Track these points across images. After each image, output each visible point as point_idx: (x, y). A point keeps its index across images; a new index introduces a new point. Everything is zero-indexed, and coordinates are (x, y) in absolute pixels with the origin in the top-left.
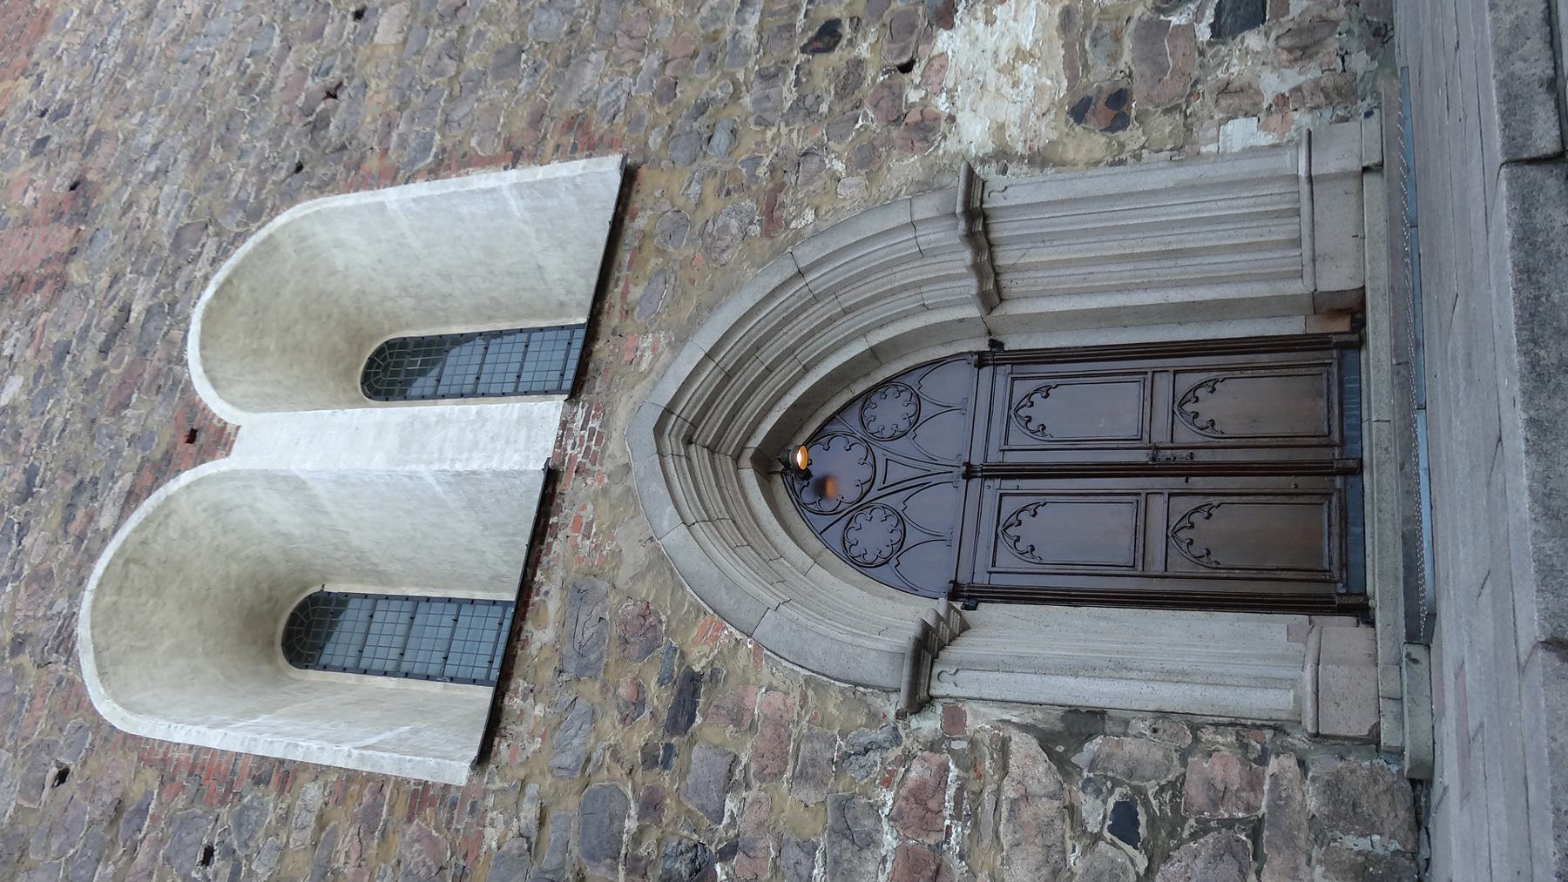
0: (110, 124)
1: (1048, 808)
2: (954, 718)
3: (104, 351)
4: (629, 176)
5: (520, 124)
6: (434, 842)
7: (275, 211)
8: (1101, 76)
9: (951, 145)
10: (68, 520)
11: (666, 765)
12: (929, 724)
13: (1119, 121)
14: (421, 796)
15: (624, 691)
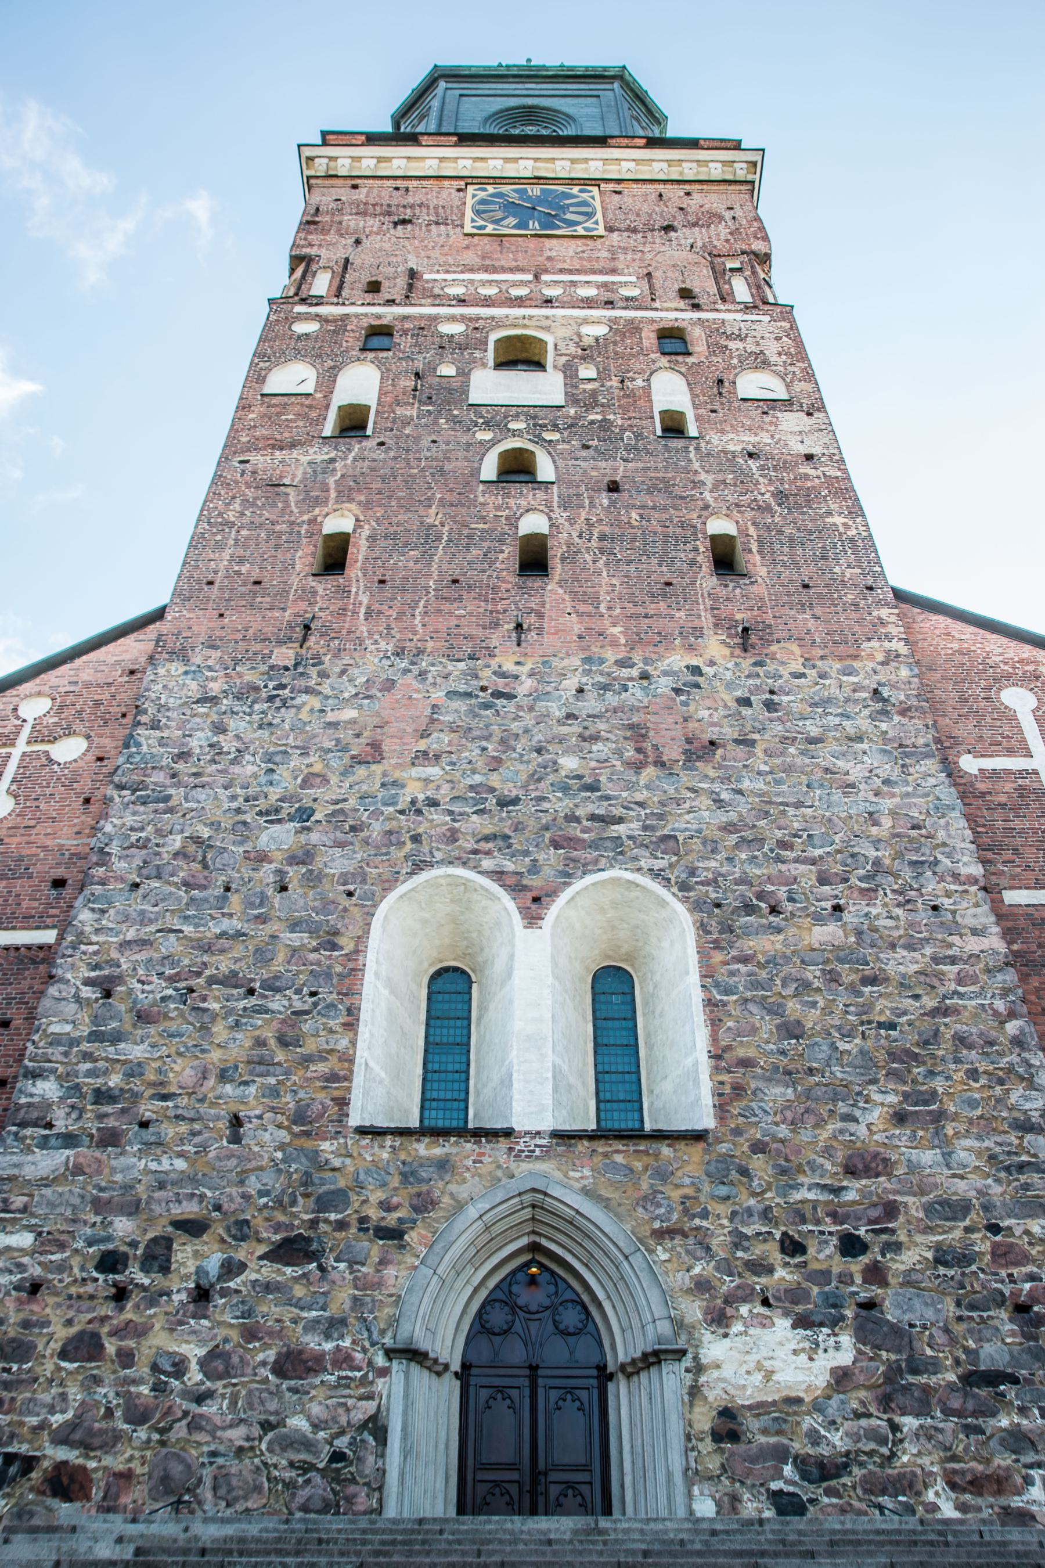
0: (759, 751)
1: (343, 1420)
2: (384, 1372)
3: (593, 817)
4: (698, 1136)
5: (741, 1053)
6: (322, 1115)
7: (685, 900)
8: (752, 1424)
9: (707, 1336)
10: (487, 838)
11: (360, 1230)
12: (380, 1361)
13: (717, 1436)
14: (343, 1103)
15: (395, 1200)
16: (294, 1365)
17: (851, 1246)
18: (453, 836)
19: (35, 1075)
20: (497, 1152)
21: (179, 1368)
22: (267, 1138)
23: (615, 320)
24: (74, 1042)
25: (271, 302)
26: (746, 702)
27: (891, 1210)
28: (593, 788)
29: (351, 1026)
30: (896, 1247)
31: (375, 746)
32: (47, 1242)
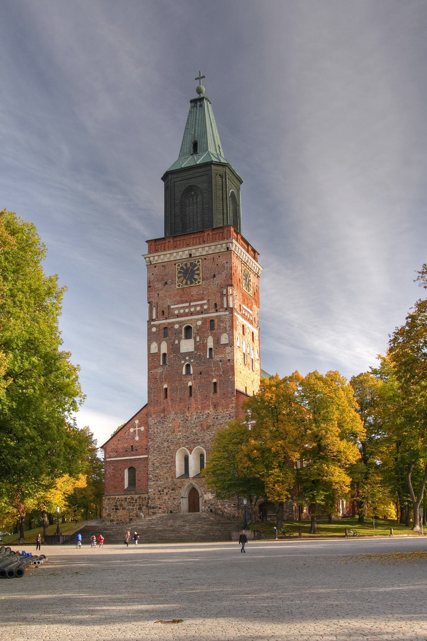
14: (175, 475)
16: (174, 499)
20: (188, 479)
21: (166, 499)
23: (203, 319)
25: (147, 321)
26: (214, 418)
28: (196, 434)
29: (175, 467)
31: (174, 430)
32: (154, 490)
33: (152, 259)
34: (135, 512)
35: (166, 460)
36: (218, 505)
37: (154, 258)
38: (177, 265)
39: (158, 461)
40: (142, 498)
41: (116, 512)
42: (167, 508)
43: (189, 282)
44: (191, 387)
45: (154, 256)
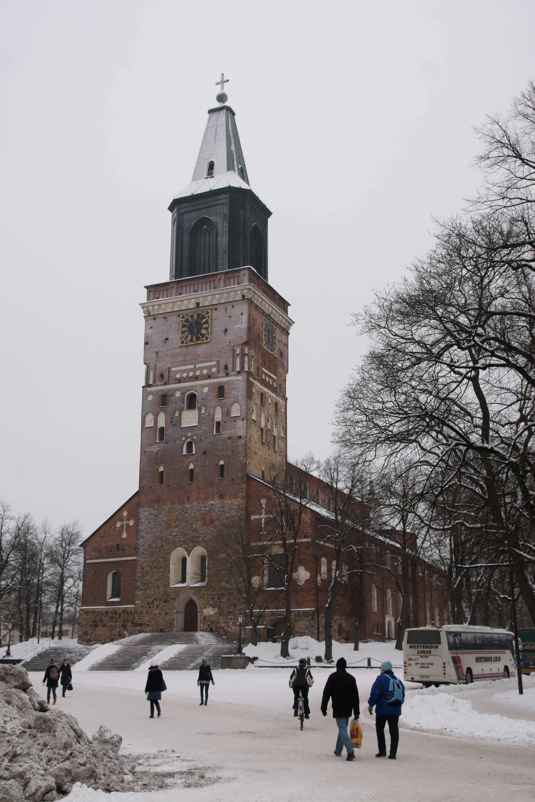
3: (197, 537)
10: (184, 542)
16: (166, 613)
17: (219, 599)
18: (179, 542)
19: (137, 582)
22: (162, 588)
24: (140, 577)
25: (143, 387)
27: (224, 594)
28: (197, 531)
29: (169, 573)
30: (223, 599)
31: (169, 525)
32: (142, 602)
33: (150, 308)
34: (117, 630)
35: (159, 563)
36: (220, 623)
37: (153, 309)
38: (181, 316)
39: (149, 564)
40: (127, 612)
41: (95, 629)
42: (157, 625)
43: (194, 339)
44: (192, 470)
45: (154, 305)
